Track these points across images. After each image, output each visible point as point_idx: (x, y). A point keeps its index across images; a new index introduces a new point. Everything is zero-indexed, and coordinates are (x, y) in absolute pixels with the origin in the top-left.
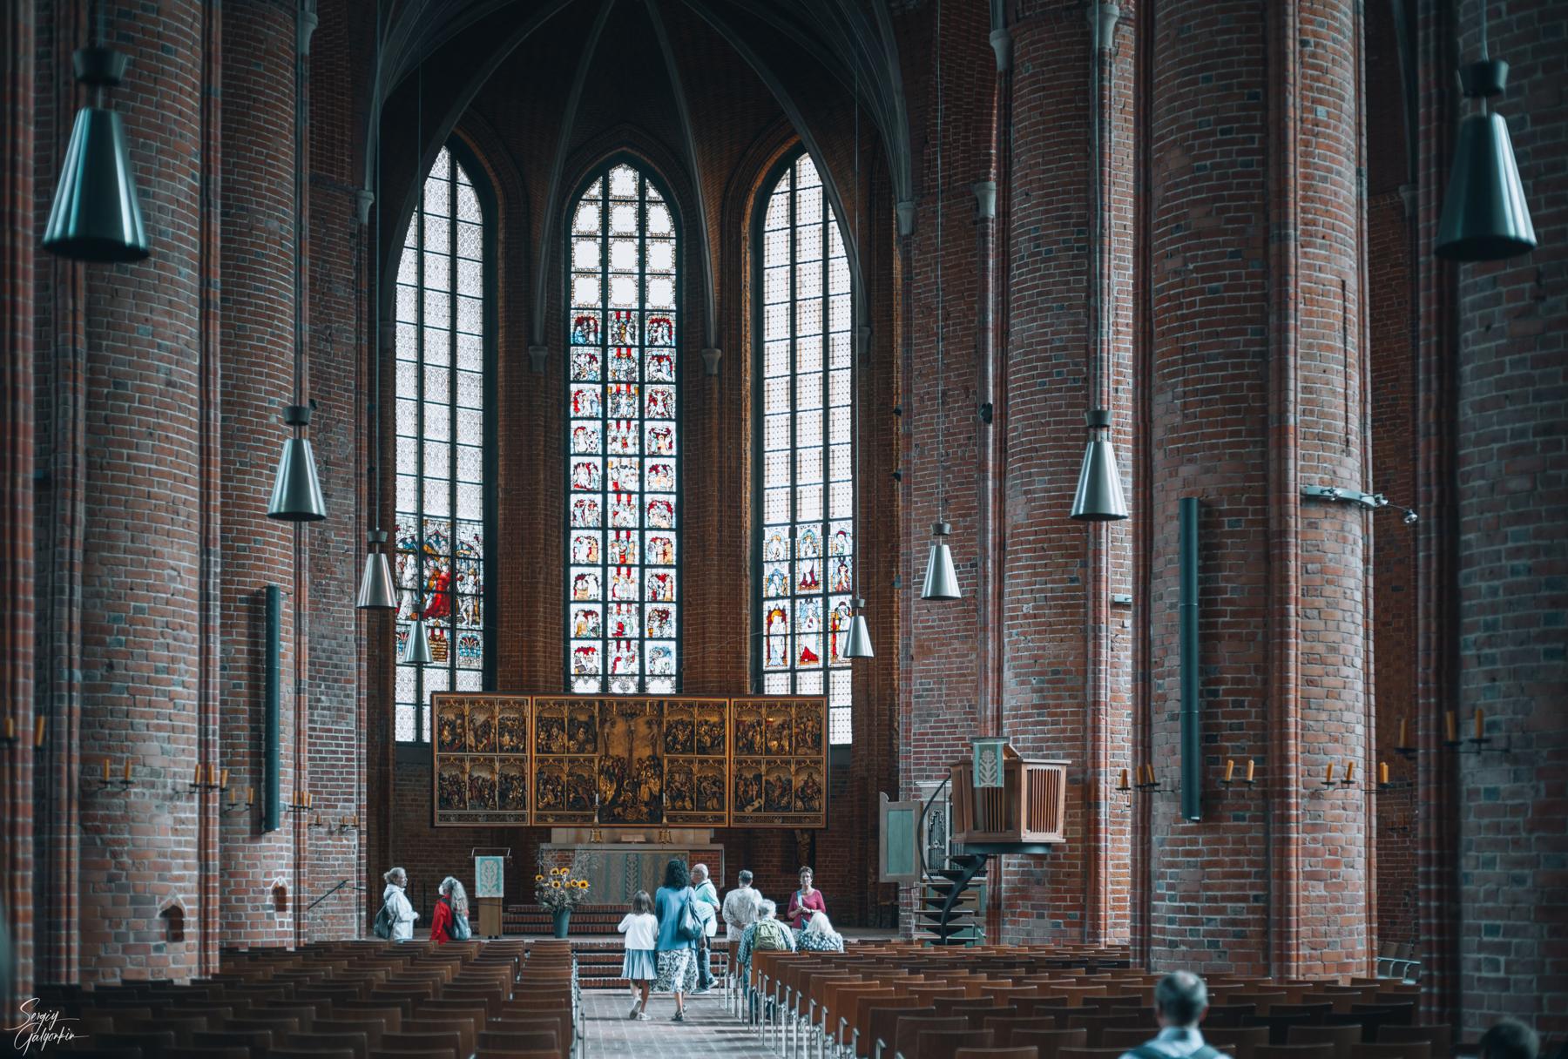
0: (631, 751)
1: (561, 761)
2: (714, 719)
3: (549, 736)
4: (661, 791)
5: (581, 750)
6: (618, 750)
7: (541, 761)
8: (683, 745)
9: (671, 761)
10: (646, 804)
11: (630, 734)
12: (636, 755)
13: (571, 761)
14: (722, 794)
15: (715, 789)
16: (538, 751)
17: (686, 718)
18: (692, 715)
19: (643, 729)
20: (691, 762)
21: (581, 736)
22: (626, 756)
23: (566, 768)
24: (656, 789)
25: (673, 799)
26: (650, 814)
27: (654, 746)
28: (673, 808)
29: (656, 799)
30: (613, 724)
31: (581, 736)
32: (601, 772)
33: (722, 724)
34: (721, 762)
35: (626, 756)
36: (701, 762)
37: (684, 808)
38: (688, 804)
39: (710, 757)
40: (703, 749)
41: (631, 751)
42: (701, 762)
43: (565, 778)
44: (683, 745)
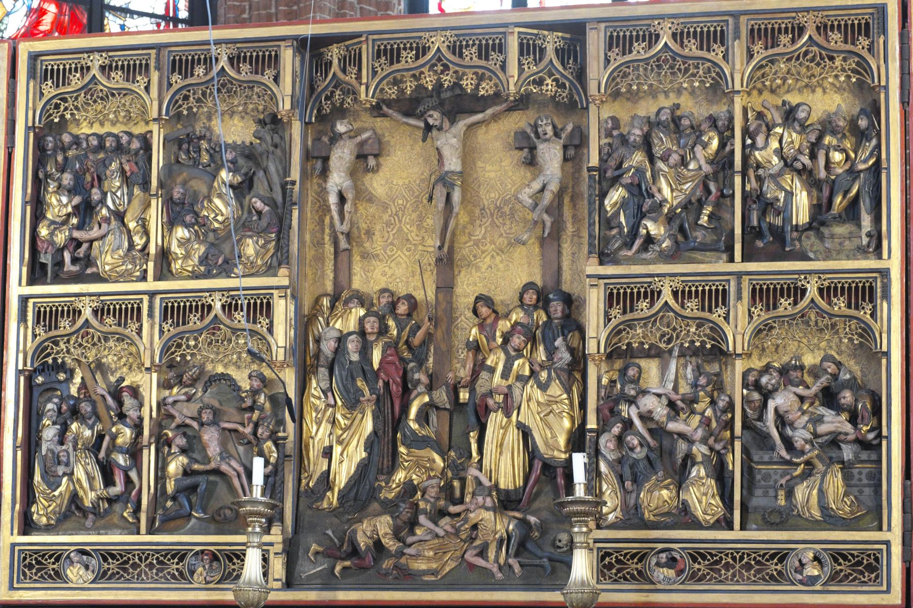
0: (447, 263)
1: (128, 313)
2: (827, 101)
3: (86, 211)
4: (577, 440)
5: (218, 262)
6: (394, 268)
7: (48, 317)
8: (681, 222)
9: (620, 298)
10: (507, 502)
11: (446, 190)
12: (467, 288)
13: (175, 312)
14: (872, 446)
15: (834, 422)
16: (37, 273)
17: (694, 108)
18: (718, 88)
19: (499, 172)
20: (717, 297)
21: (221, 209)
22: (425, 291)
23: (151, 337)
24: (554, 437)
25: (631, 475)
26: (522, 544)
27: (551, 240)
28: (633, 517)
29: (549, 474)
30: (366, 158)
31: (221, 209)
32: (306, 363)
33: (865, 128)
34: (864, 293)
35: (425, 291)
36: (765, 295)
37: (683, 517)
38: (701, 496)
39: (814, 268)
40: (769, 236)
41: (447, 263)
42: (765, 295)
43: (151, 394)
44: (681, 222)
